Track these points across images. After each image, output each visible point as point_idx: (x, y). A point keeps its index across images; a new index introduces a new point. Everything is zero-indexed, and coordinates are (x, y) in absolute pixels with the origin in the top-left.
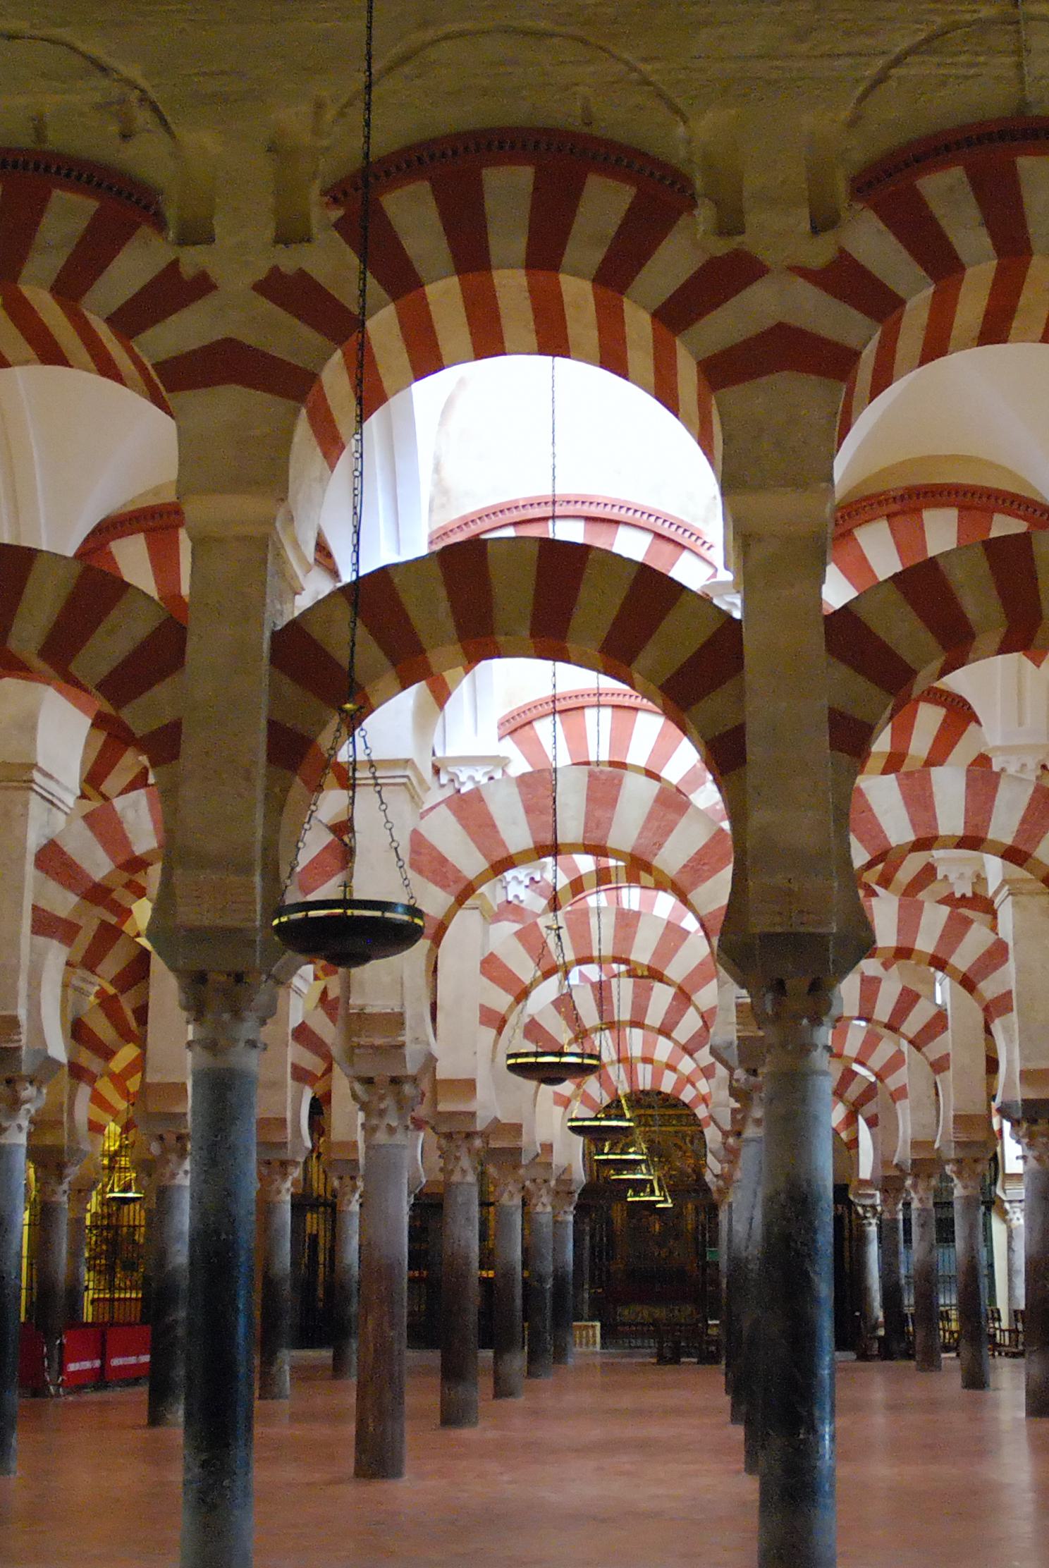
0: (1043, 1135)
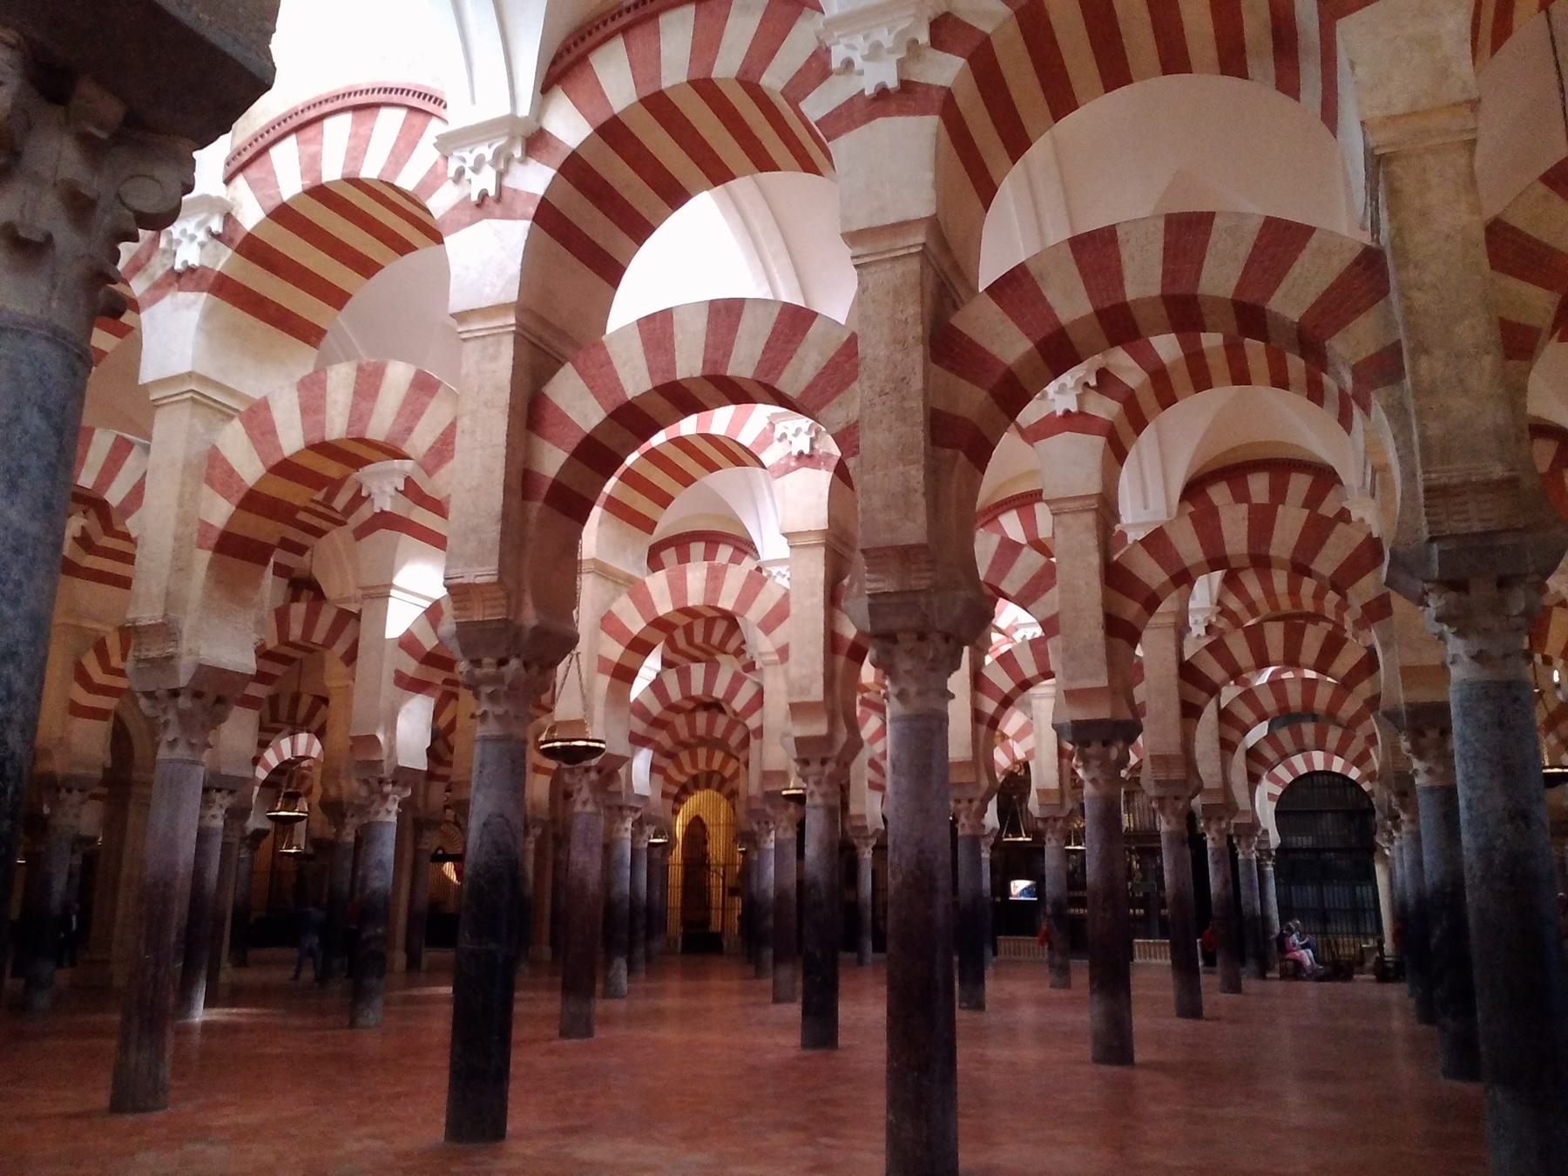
0: (1097, 758)
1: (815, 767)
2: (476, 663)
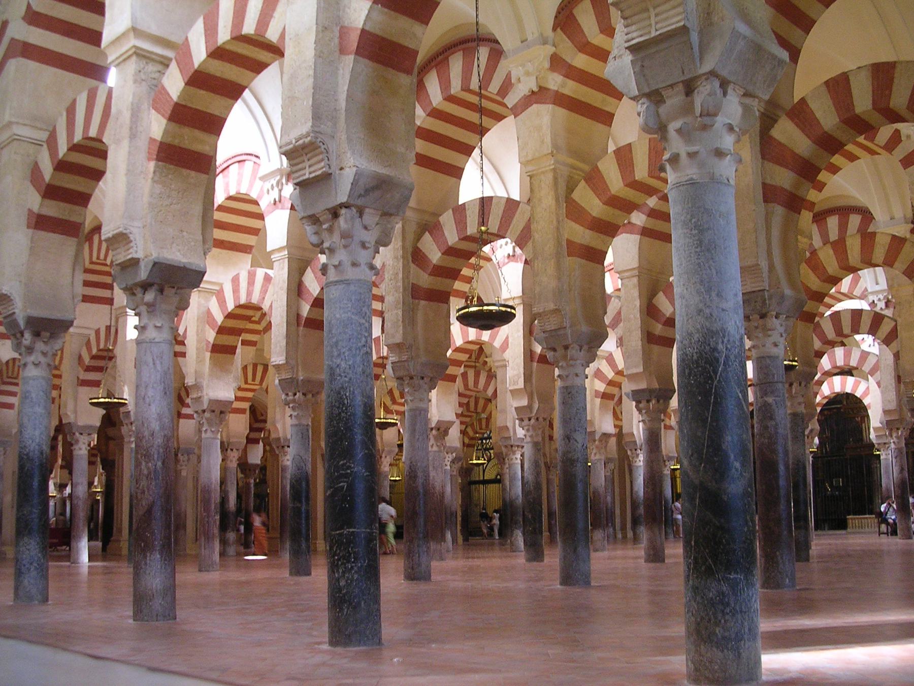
1: (526, 422)
2: (287, 395)
